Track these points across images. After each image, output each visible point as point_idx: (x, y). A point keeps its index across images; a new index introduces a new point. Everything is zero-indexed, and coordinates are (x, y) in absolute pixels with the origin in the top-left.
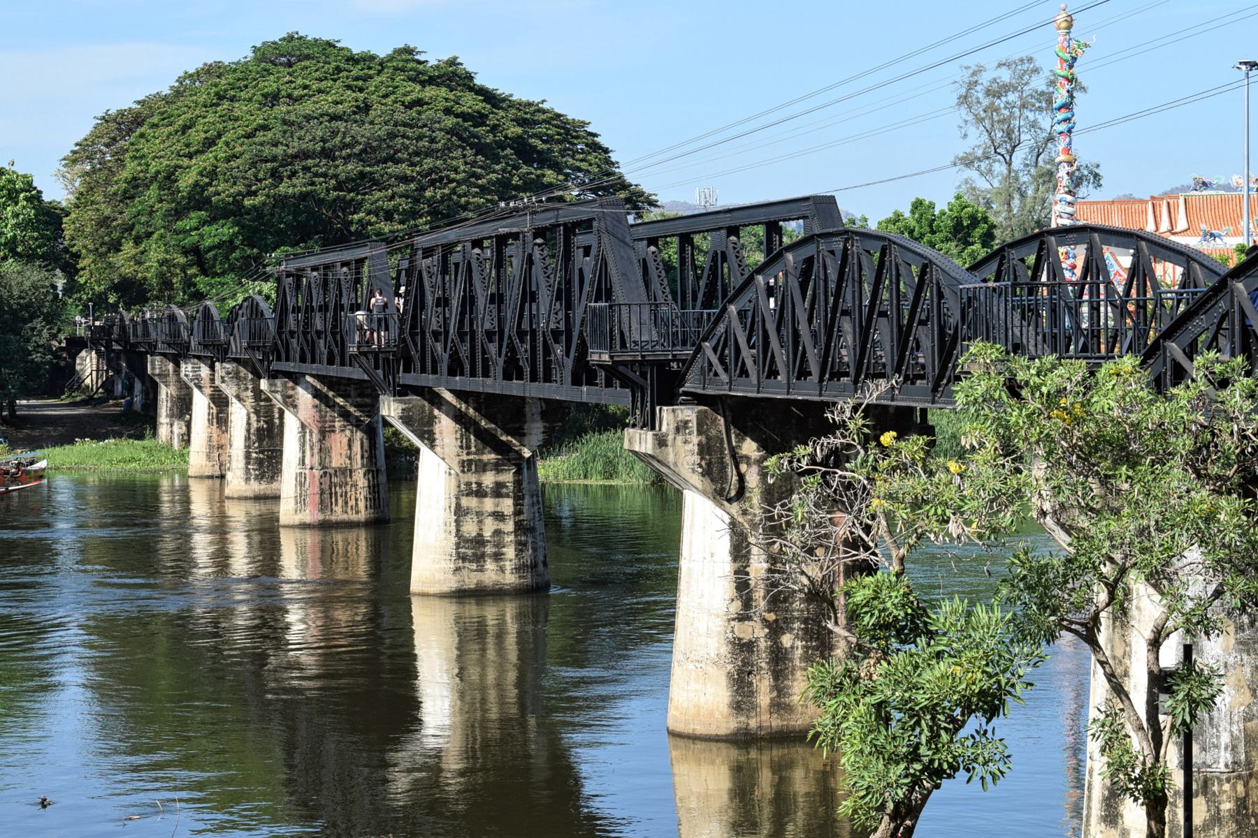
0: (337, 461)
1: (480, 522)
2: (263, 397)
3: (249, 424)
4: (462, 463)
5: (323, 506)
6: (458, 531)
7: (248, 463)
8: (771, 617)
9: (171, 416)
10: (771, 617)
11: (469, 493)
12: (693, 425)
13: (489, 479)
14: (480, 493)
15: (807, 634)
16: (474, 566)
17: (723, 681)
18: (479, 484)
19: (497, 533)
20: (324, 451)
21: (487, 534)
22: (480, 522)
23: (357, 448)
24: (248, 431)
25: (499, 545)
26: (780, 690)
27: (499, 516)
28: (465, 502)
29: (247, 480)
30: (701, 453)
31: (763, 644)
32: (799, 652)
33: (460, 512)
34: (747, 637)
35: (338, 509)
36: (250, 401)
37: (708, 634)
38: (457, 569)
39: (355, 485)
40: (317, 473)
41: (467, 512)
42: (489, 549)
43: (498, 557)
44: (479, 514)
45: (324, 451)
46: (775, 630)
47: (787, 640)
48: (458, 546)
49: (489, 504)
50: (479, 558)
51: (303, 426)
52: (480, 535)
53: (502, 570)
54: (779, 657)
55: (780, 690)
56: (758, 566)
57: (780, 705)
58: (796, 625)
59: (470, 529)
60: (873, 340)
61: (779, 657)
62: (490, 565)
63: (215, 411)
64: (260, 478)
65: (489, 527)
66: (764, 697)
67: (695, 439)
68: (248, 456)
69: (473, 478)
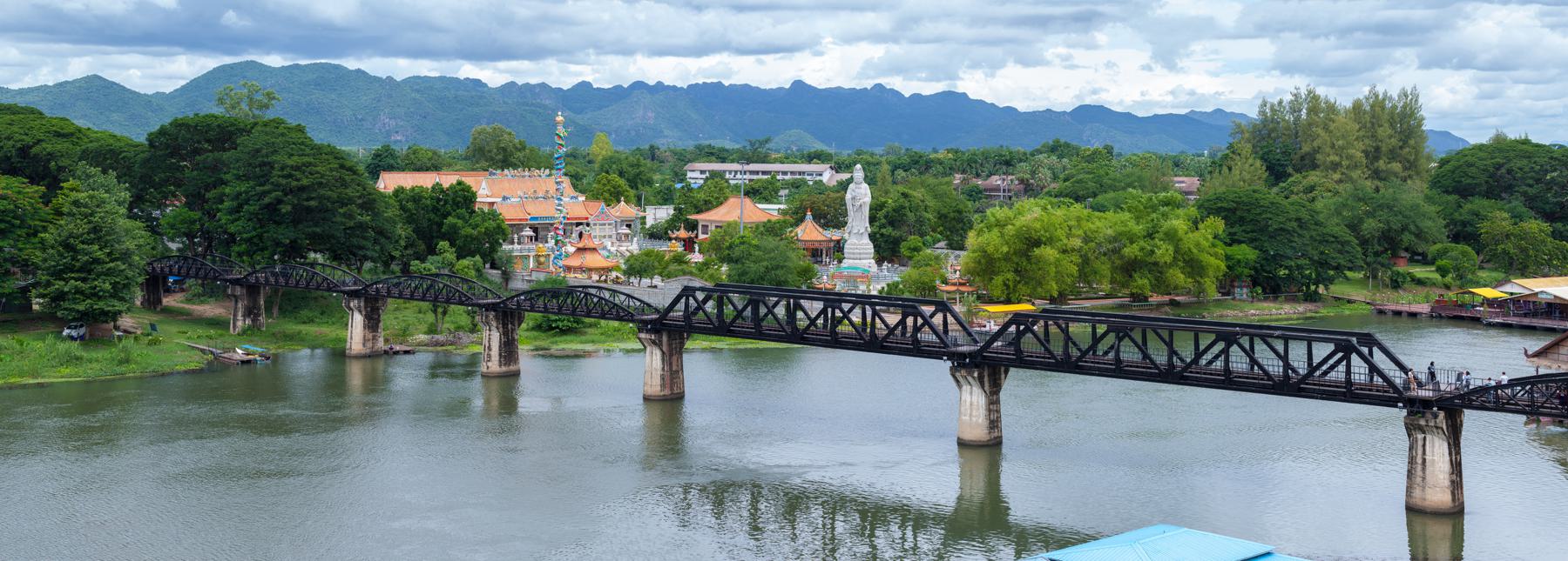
2: (120, 286)
3: (500, 339)
5: (672, 389)
7: (500, 358)
9: (244, 316)
17: (1450, 493)
24: (500, 342)
28: (991, 407)
29: (500, 366)
33: (990, 411)
36: (501, 330)
37: (1444, 479)
51: (663, 353)
56: (1454, 457)
63: (367, 322)
64: (505, 365)
68: (500, 355)
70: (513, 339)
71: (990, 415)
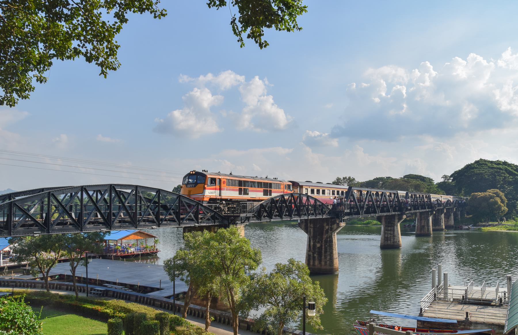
0: (423, 224)
1: (388, 235)
4: (385, 226)
5: (421, 231)
6: (385, 236)
8: (313, 251)
10: (313, 251)
11: (386, 230)
12: (304, 222)
13: (389, 228)
14: (388, 230)
15: (318, 255)
18: (388, 229)
19: (390, 236)
20: (421, 223)
21: (389, 237)
22: (388, 235)
23: (426, 222)
25: (391, 238)
26: (314, 262)
27: (390, 234)
28: (386, 231)
30: (305, 226)
31: (312, 255)
32: (317, 257)
34: (310, 254)
35: (422, 232)
38: (384, 242)
39: (425, 228)
40: (420, 226)
41: (386, 233)
42: (389, 239)
43: (390, 240)
45: (421, 223)
46: (314, 253)
47: (315, 255)
48: (384, 238)
49: (389, 232)
50: (388, 240)
52: (388, 237)
53: (391, 242)
54: (314, 257)
55: (314, 262)
56: (312, 243)
57: (314, 265)
58: (317, 253)
59: (386, 236)
60: (312, 211)
61: (314, 257)
62: (389, 242)
64: (434, 226)
65: (389, 236)
66: (311, 263)
67: (304, 224)
69: (387, 228)
70: (438, 219)
71: (385, 235)
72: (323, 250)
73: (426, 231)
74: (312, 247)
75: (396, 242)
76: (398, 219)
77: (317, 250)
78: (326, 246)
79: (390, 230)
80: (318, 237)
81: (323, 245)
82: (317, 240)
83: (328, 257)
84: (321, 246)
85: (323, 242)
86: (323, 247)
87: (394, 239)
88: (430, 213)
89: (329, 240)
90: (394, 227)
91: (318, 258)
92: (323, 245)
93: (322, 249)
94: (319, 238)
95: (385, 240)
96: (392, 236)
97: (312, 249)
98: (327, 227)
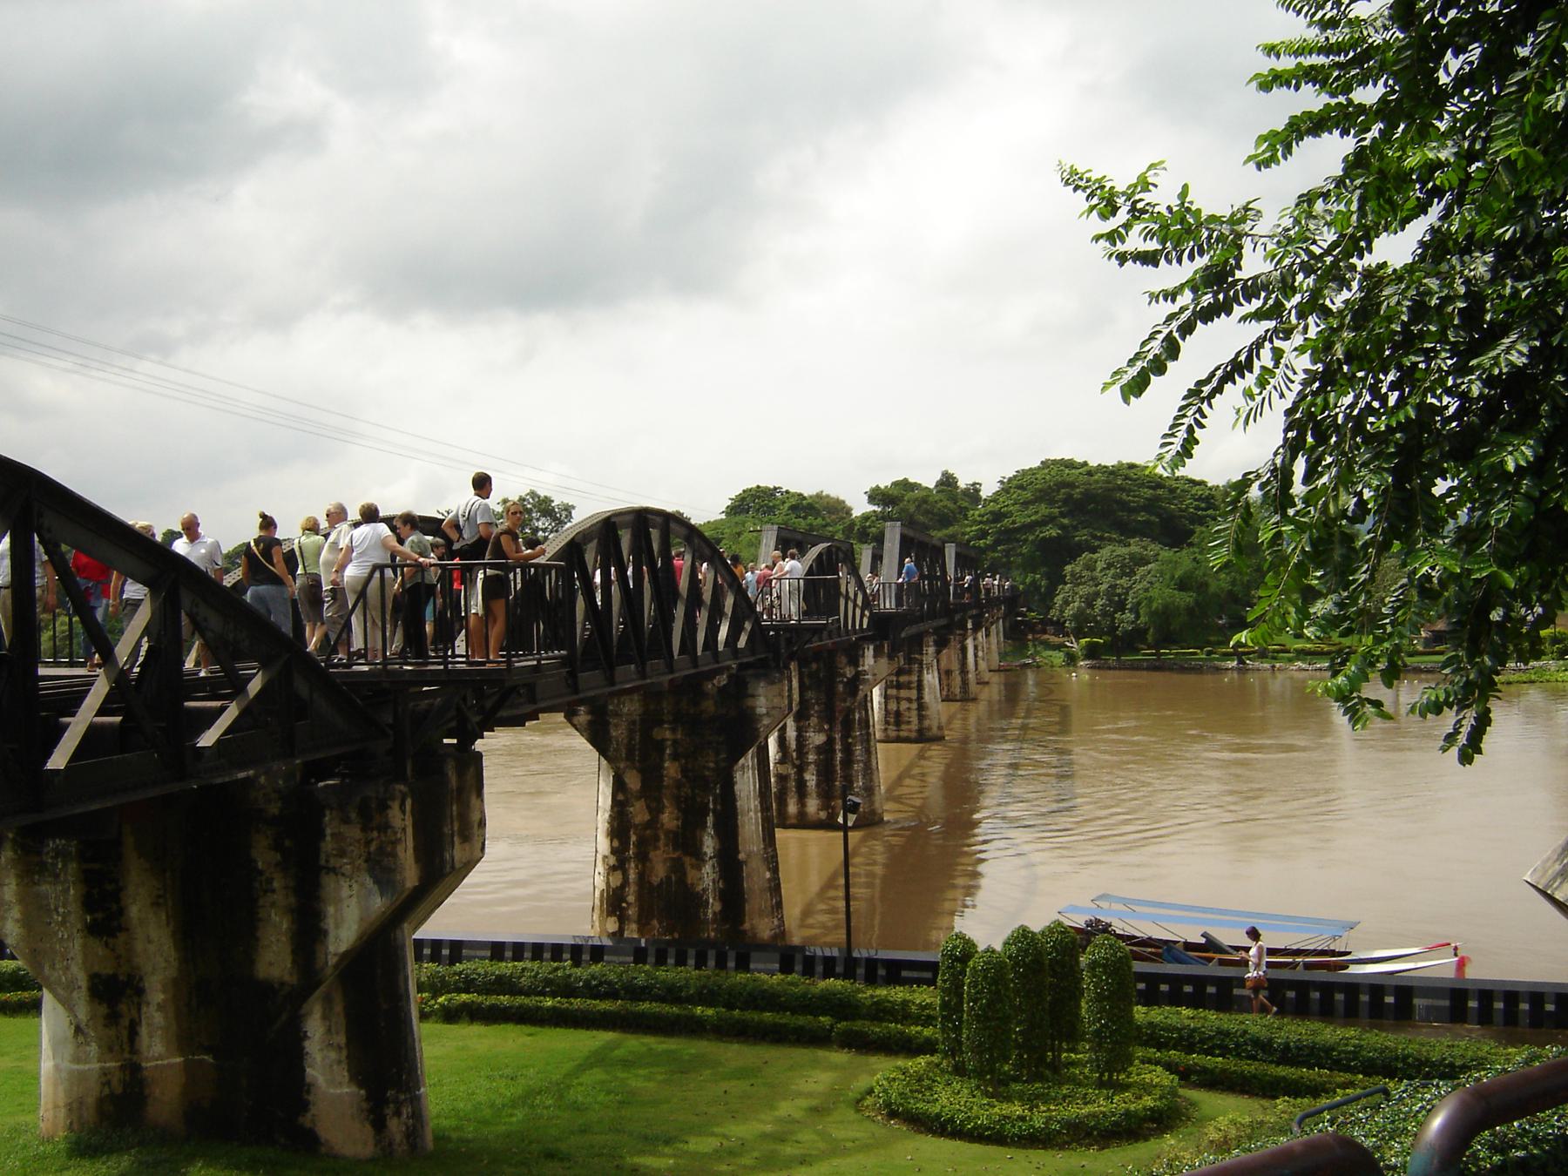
1: (898, 703)
8: (797, 762)
10: (797, 762)
14: (899, 686)
16: (894, 728)
22: (898, 703)
28: (889, 691)
34: (785, 773)
38: (886, 729)
44: (898, 699)
47: (807, 776)
49: (904, 693)
59: (893, 706)
71: (886, 704)
72: (839, 755)
73: (957, 691)
74: (793, 745)
75: (929, 729)
76: (936, 643)
77: (811, 757)
78: (850, 740)
79: (908, 686)
80: (816, 708)
81: (838, 736)
82: (814, 721)
83: (859, 783)
84: (830, 741)
85: (839, 727)
86: (838, 747)
87: (921, 718)
88: (970, 625)
89: (857, 716)
90: (920, 672)
91: (818, 785)
92: (838, 736)
93: (834, 751)
94: (816, 712)
95: (887, 723)
96: (915, 706)
97: (794, 754)
98: (849, 672)
